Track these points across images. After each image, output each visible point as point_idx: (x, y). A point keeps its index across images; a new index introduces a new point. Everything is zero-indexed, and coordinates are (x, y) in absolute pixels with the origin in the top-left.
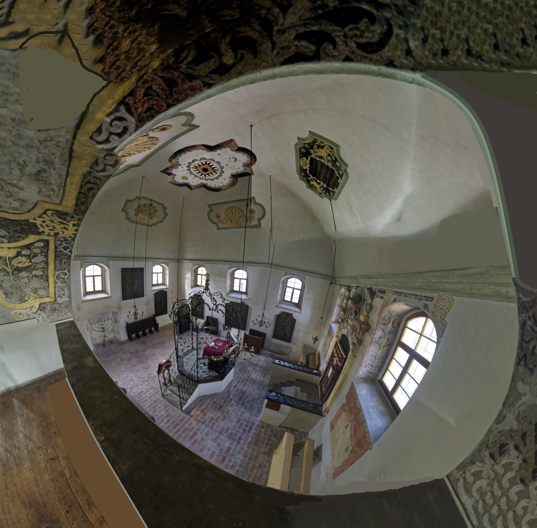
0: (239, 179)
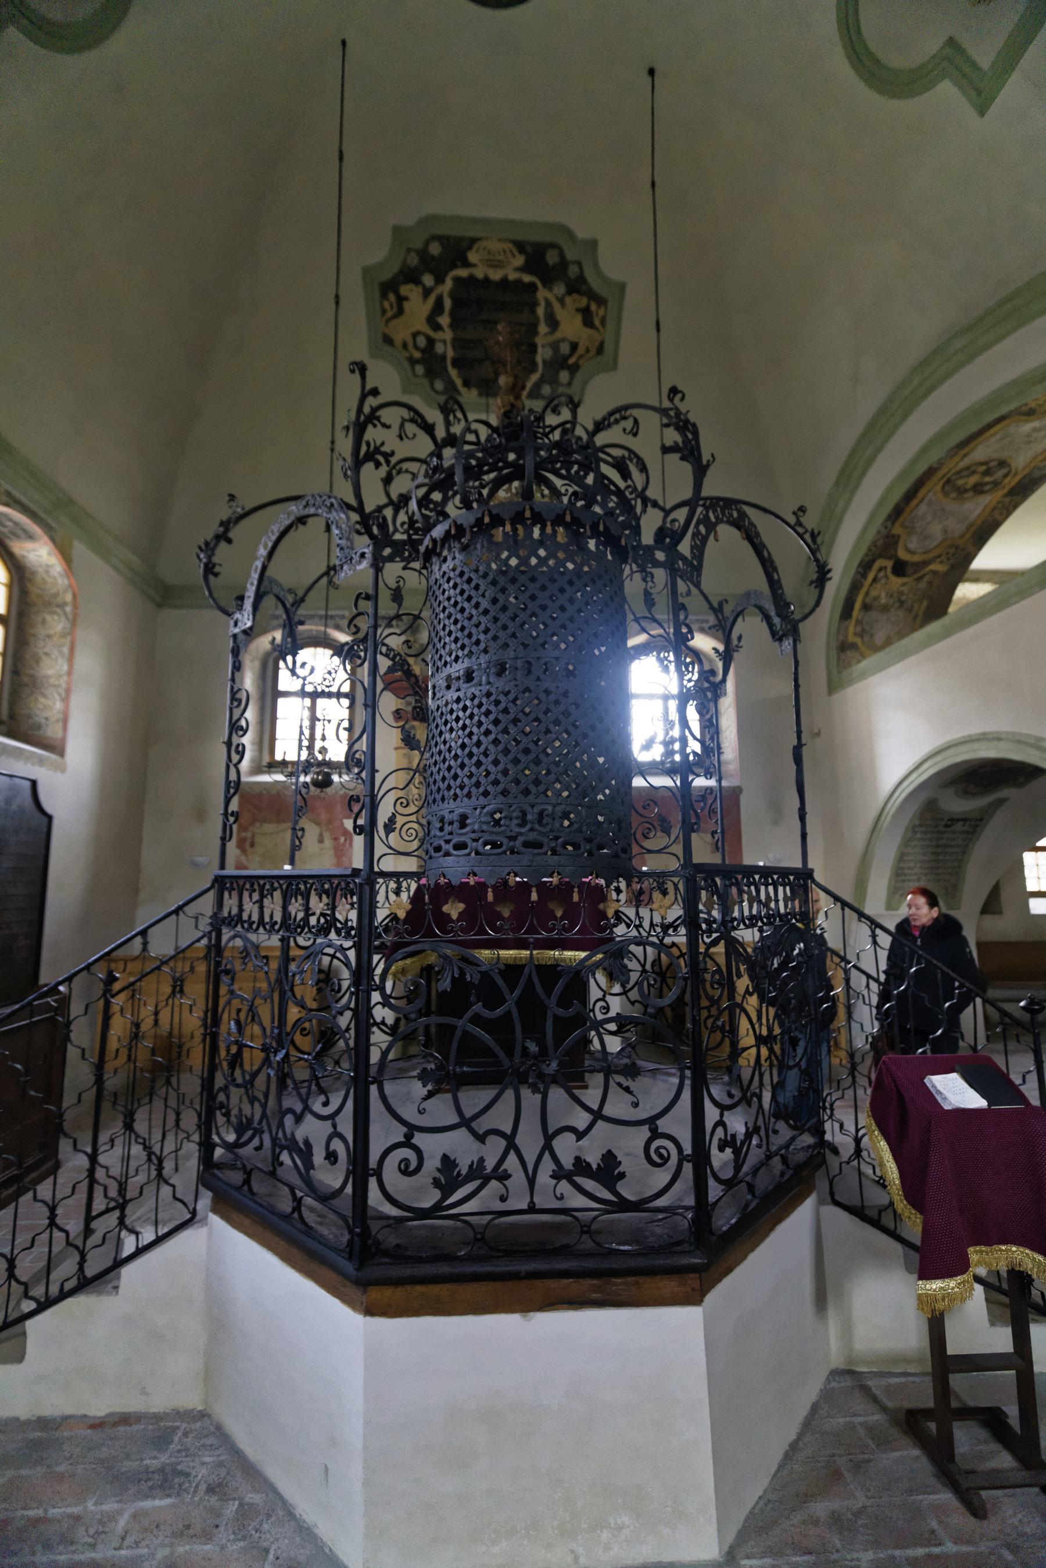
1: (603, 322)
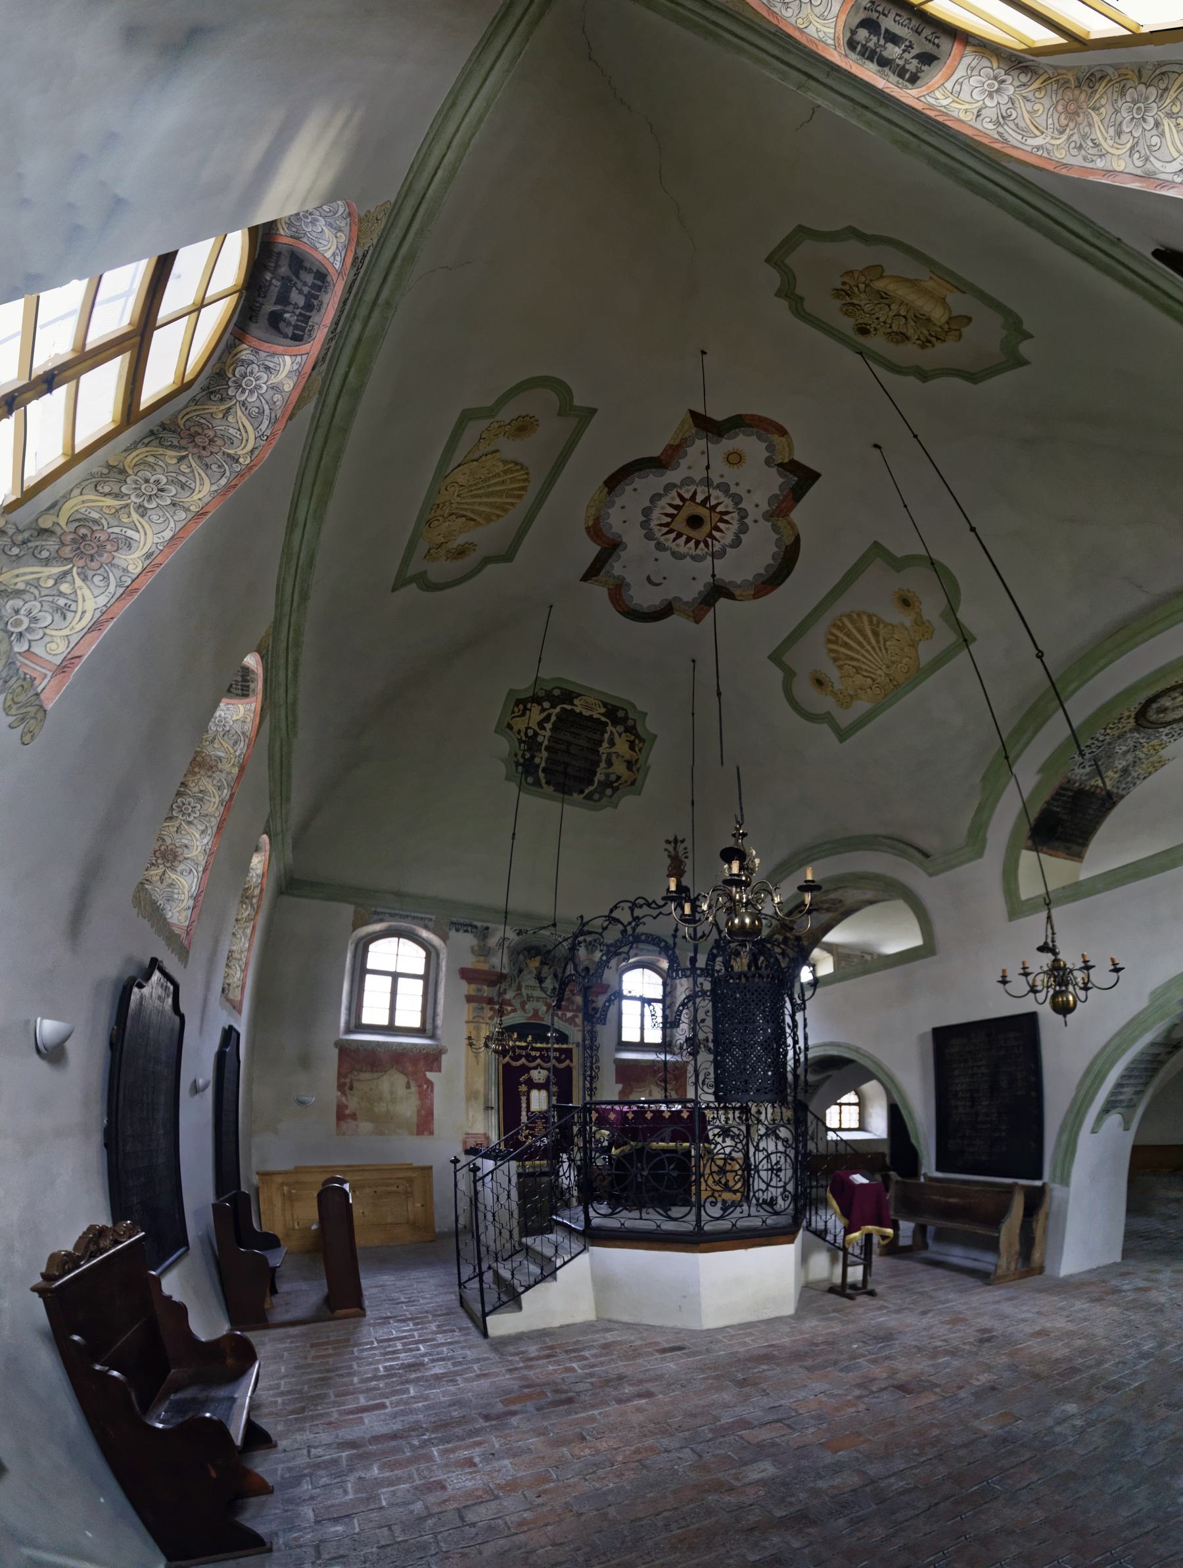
0: (595, 549)
1: (640, 750)
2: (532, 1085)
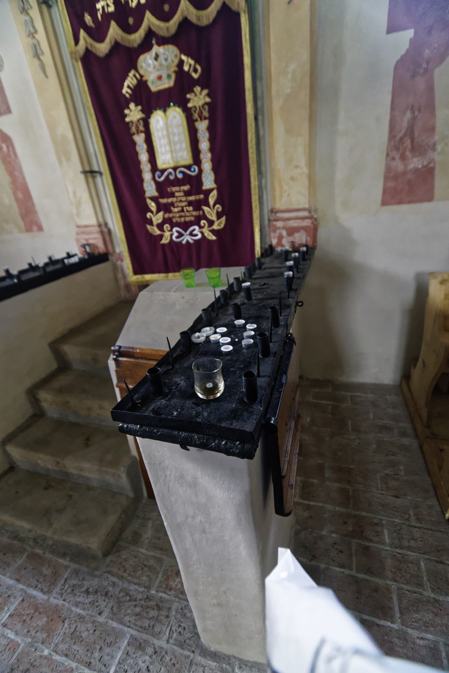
2: (151, 102)
